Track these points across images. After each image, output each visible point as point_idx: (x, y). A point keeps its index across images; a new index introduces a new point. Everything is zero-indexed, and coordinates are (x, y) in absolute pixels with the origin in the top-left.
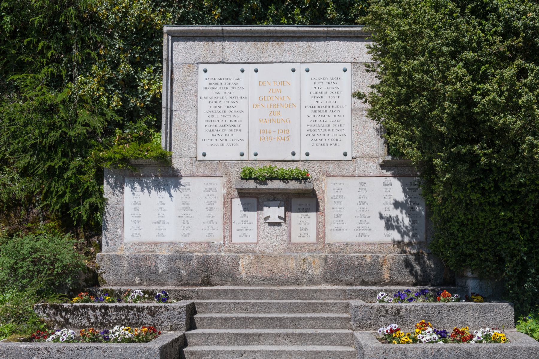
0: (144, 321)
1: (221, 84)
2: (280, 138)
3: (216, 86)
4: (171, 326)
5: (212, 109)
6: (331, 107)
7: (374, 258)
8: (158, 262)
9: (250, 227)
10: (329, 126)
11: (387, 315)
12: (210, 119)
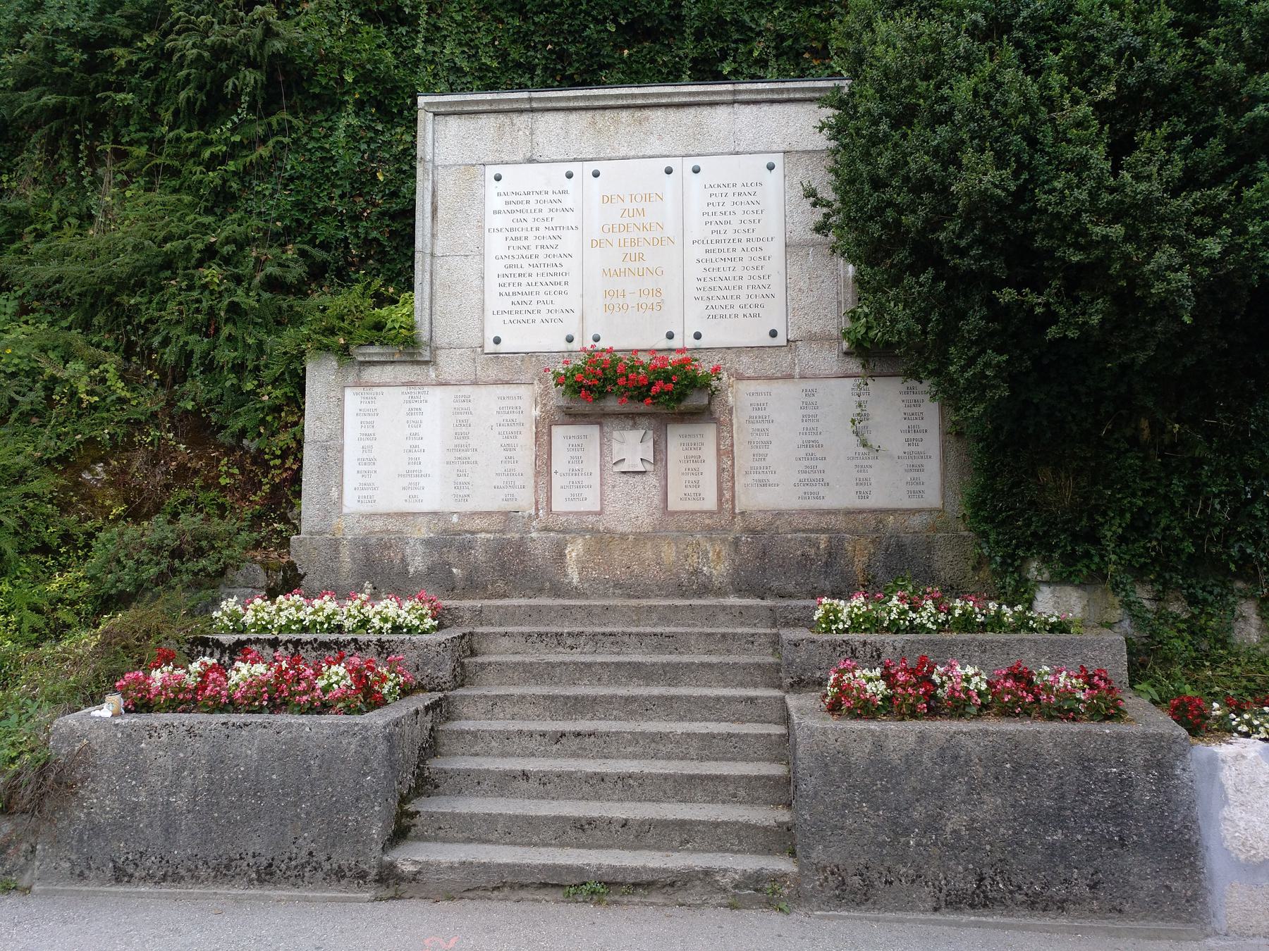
1: (528, 202)
2: (644, 307)
3: (519, 207)
5: (511, 252)
6: (744, 240)
9: (586, 481)
10: (740, 278)
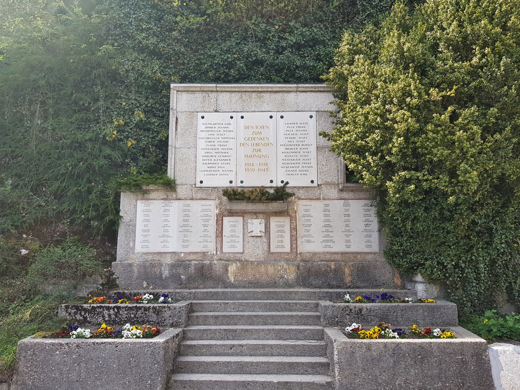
0: (150, 319)
1: (215, 127)
2: (261, 170)
3: (211, 129)
4: (173, 323)
5: (208, 147)
6: (301, 145)
7: (337, 266)
8: (163, 268)
9: (237, 239)
10: (299, 160)
11: (351, 314)
12: (206, 155)
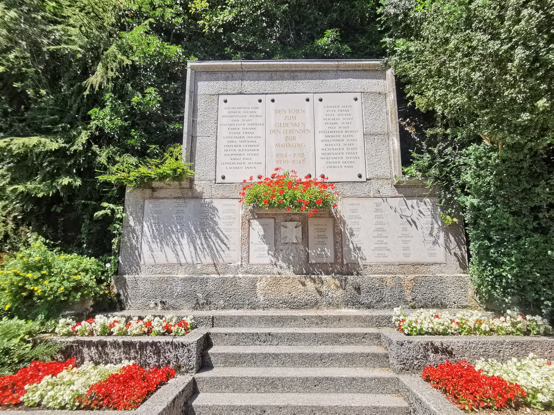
2: (296, 161)
5: (231, 135)
10: (343, 149)
